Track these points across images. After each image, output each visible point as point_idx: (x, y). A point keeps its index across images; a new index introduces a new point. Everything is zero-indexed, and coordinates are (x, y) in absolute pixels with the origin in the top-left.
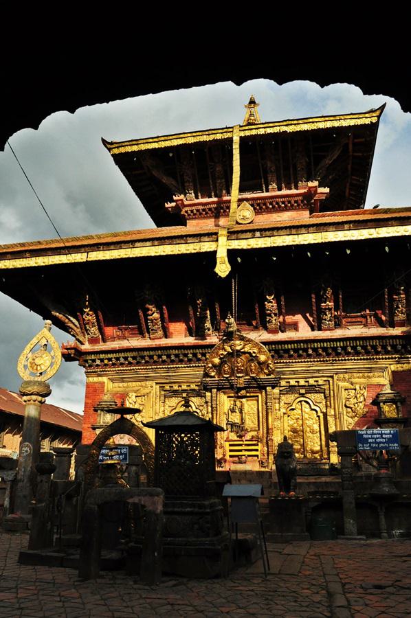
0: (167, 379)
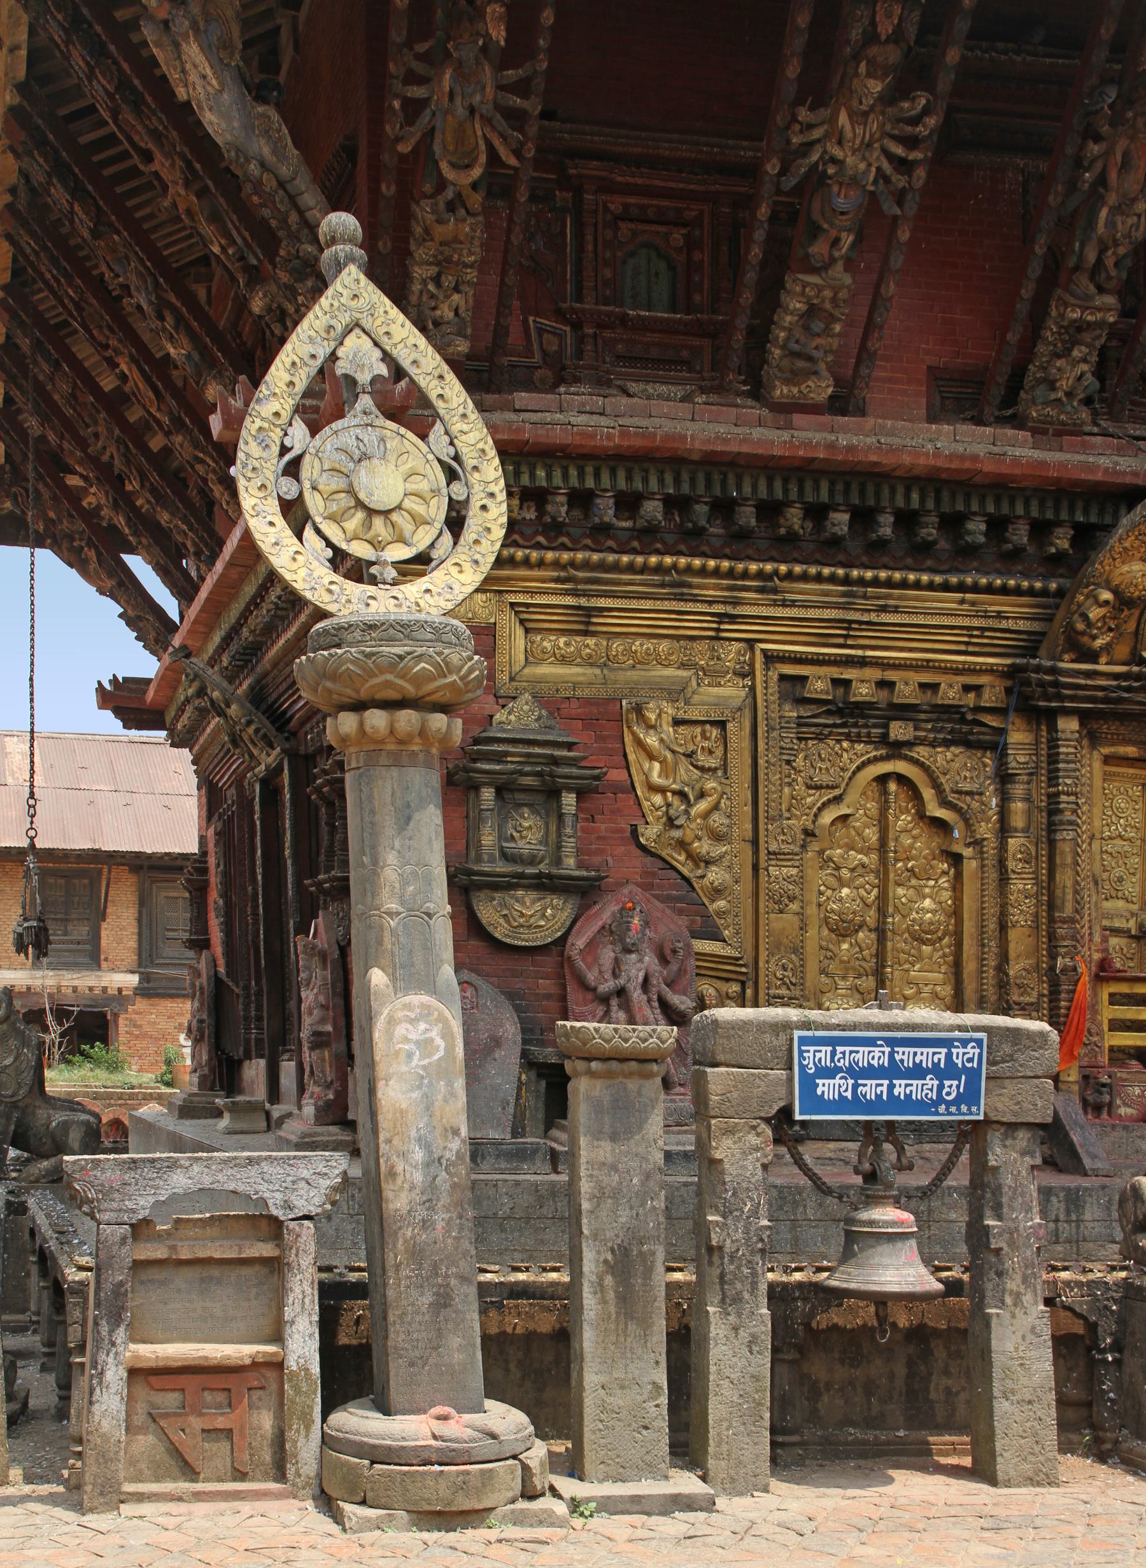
0: (823, 640)
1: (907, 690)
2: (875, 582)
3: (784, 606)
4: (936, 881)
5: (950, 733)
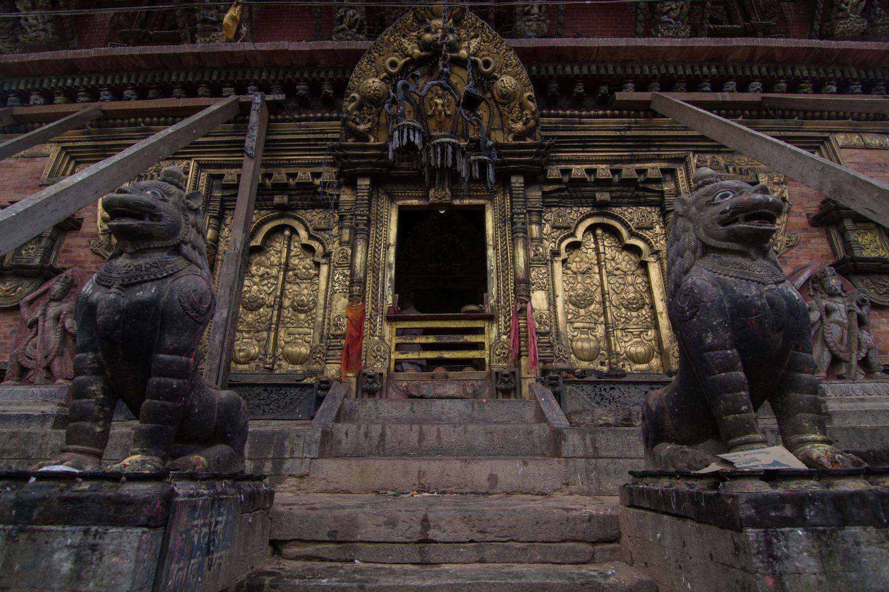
5: (311, 200)
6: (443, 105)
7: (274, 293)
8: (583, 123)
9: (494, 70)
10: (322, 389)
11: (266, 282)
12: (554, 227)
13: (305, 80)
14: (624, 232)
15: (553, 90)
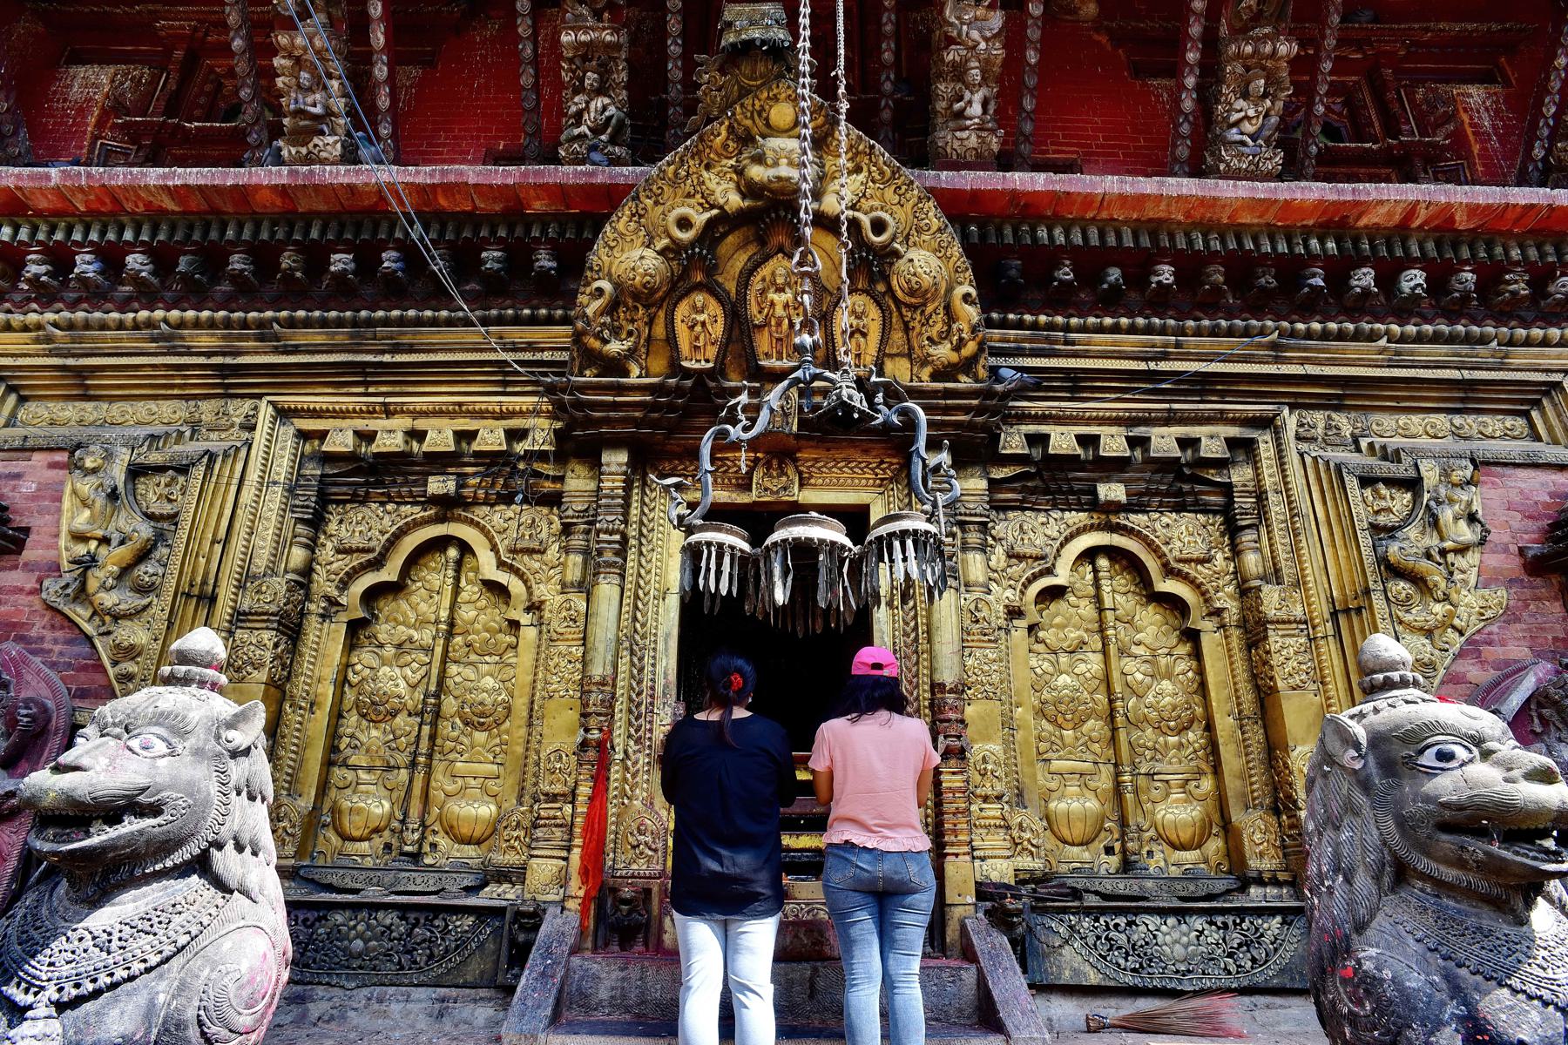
1: (440, 437)
2: (386, 322)
3: (283, 353)
4: (501, 656)
6: (786, 306)
7: (421, 689)
8: (1073, 343)
9: (894, 238)
10: (522, 928)
11: (408, 658)
12: (1014, 556)
13: (501, 241)
14: (1152, 565)
15: (1013, 272)
